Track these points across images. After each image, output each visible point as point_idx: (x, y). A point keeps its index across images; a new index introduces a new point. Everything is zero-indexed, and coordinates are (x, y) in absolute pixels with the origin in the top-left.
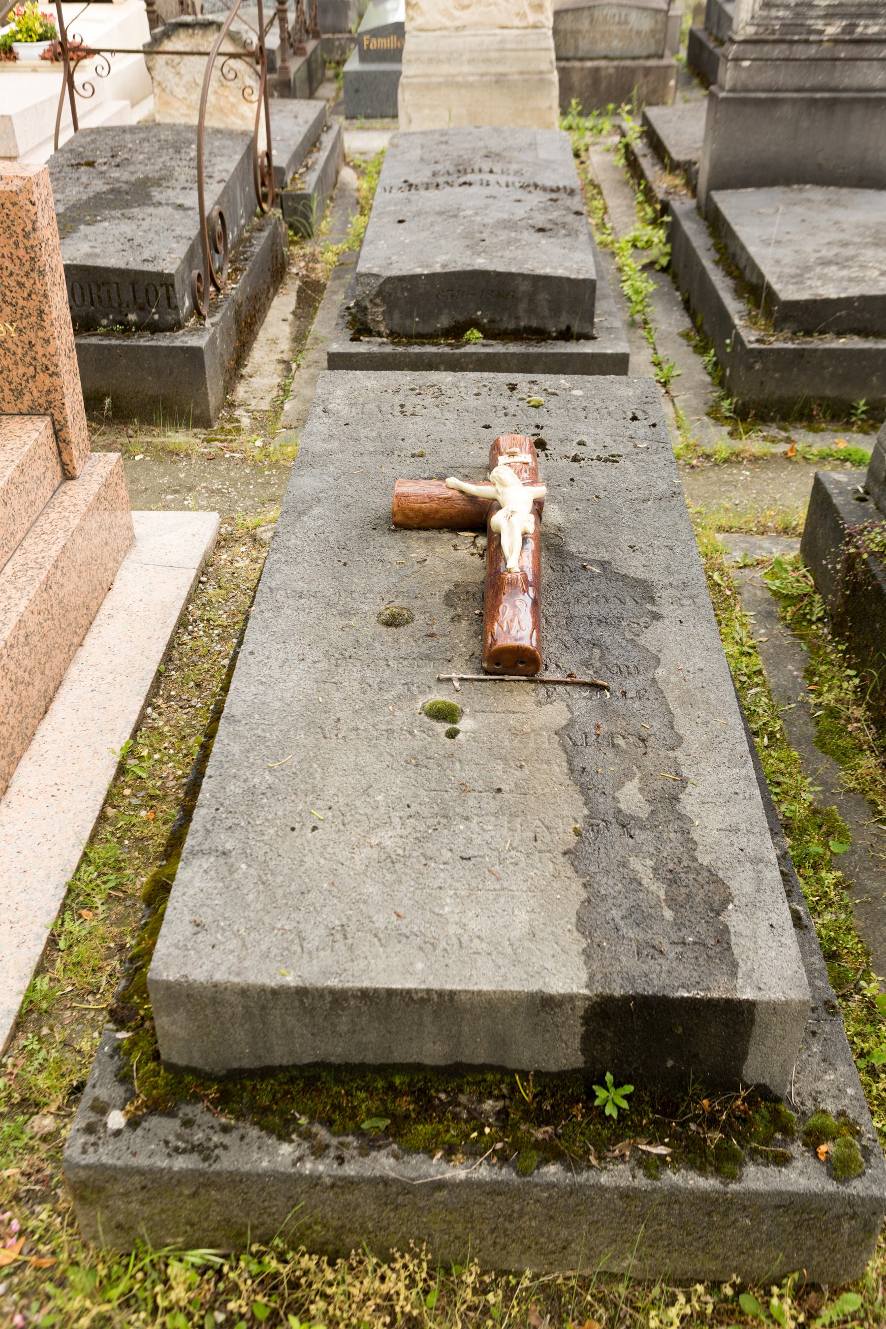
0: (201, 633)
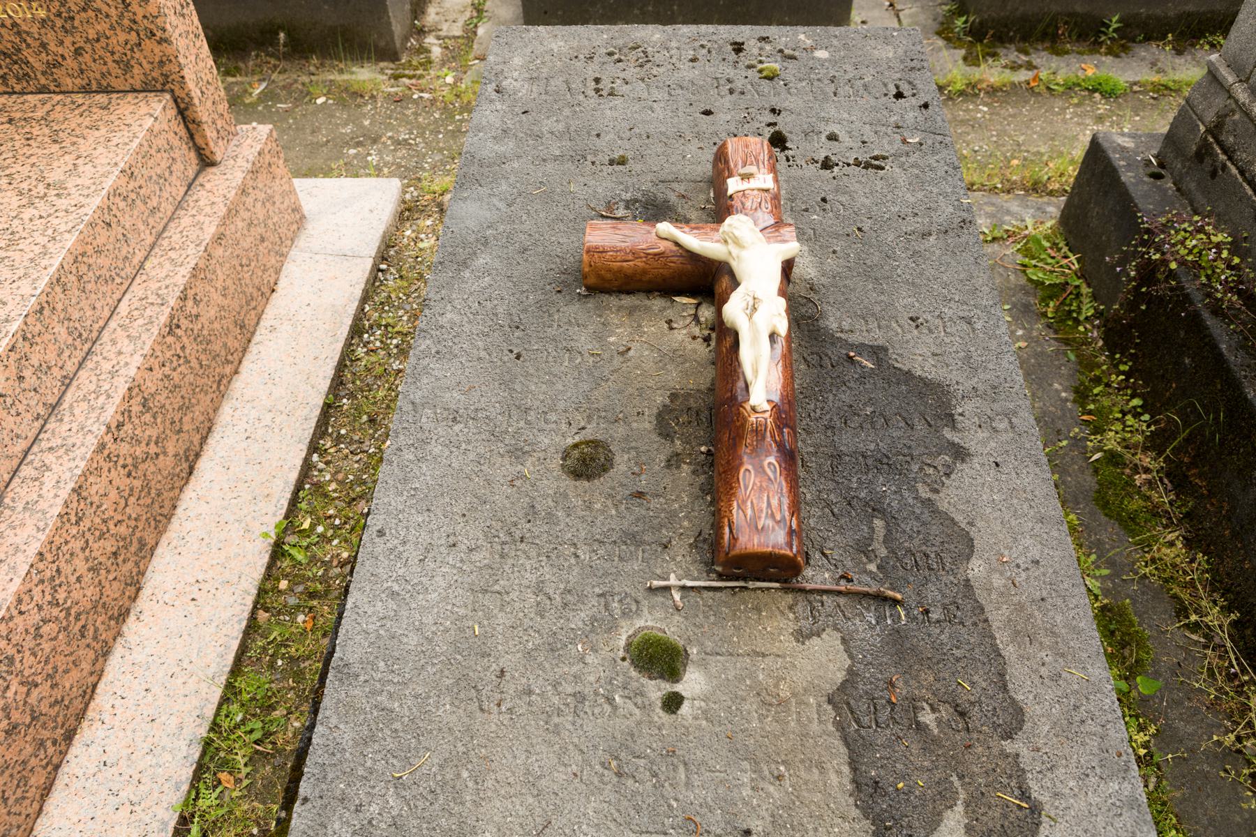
0: (378, 344)
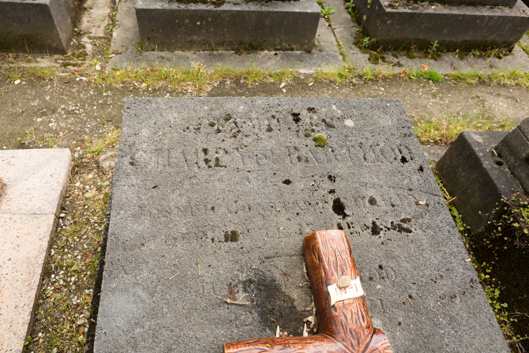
0: (62, 282)
